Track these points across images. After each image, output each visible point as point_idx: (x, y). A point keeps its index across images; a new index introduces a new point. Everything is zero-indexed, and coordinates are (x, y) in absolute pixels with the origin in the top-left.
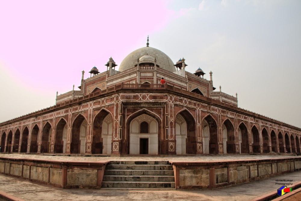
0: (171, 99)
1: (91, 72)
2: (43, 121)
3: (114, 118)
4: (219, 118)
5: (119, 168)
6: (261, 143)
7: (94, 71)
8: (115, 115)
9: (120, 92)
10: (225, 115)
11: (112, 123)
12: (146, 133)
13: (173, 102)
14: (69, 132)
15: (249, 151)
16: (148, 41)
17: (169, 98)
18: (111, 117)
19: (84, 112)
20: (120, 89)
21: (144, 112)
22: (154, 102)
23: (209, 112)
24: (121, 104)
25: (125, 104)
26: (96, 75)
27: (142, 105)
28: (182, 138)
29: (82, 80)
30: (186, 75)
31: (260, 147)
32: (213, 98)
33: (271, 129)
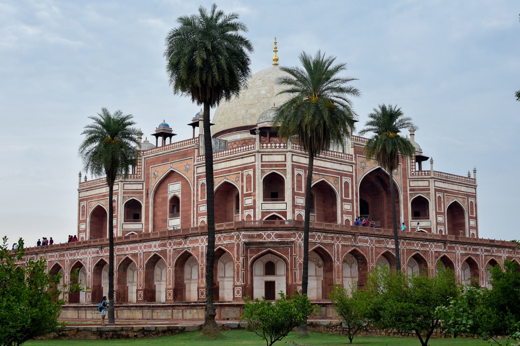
1: (157, 135)
4: (370, 252)
7: (165, 133)
8: (236, 256)
9: (242, 231)
10: (383, 245)
17: (297, 236)
19: (193, 249)
22: (281, 242)
23: (354, 246)
24: (243, 244)
25: (247, 244)
27: (267, 245)
28: (317, 280)
32: (413, 184)
33: (488, 257)
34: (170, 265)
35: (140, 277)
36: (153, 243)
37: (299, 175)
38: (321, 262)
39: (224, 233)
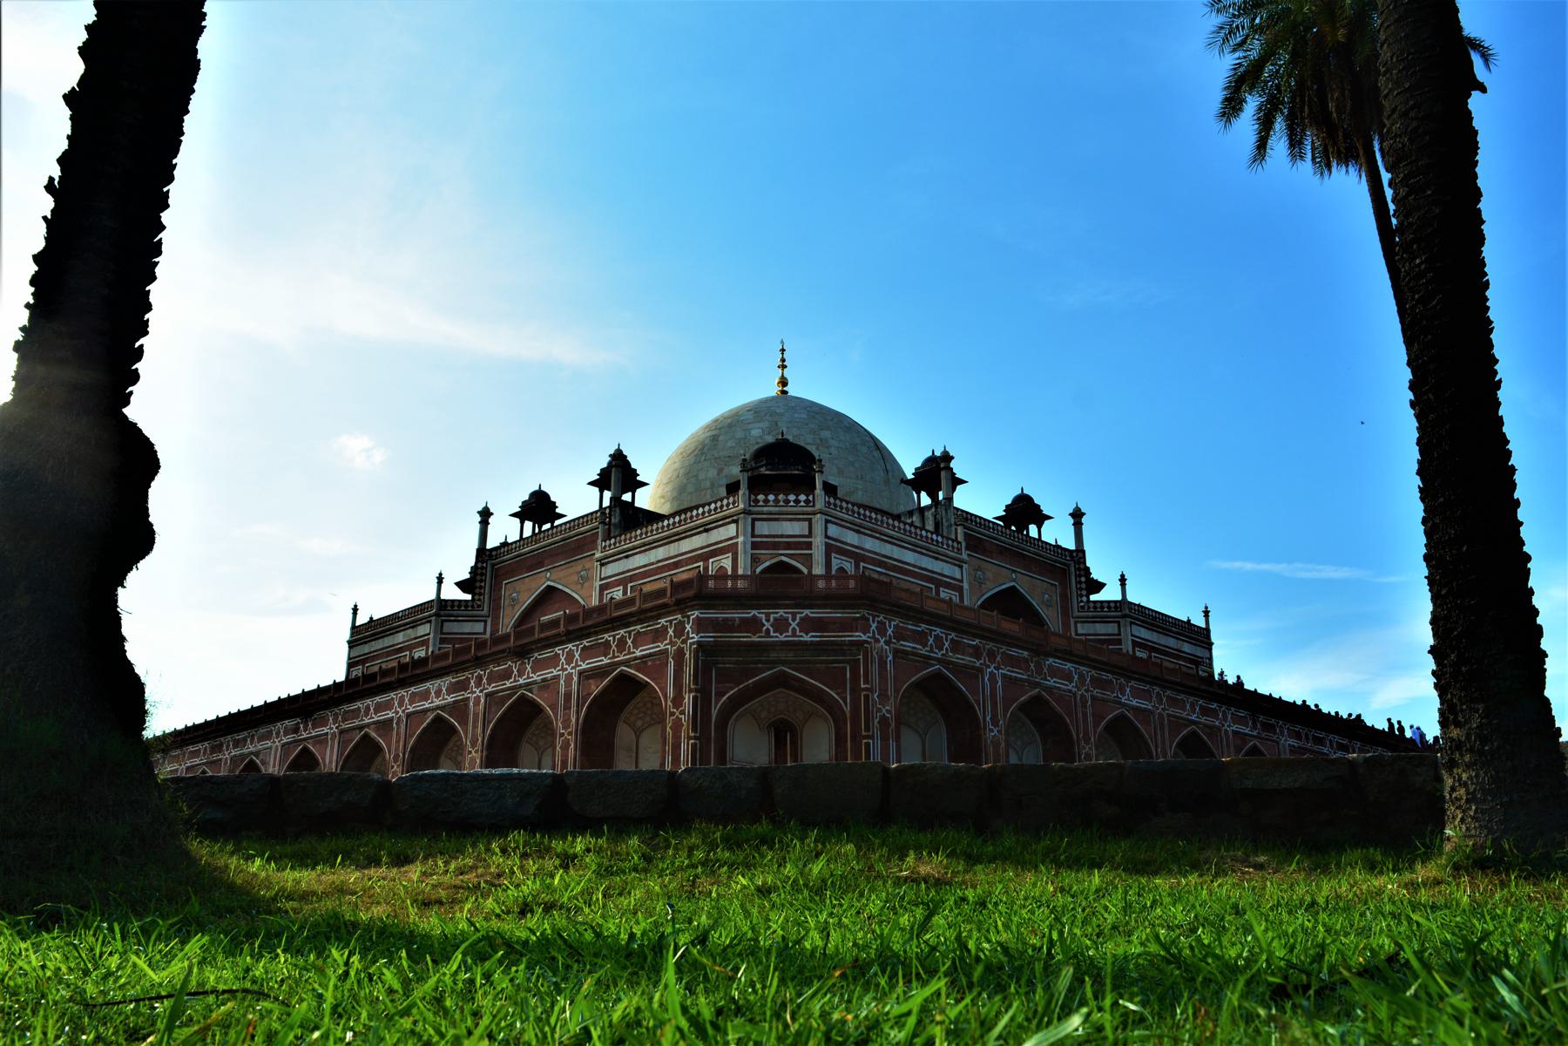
0: (882, 630)
2: (342, 732)
4: (1079, 709)
9: (693, 608)
11: (659, 727)
13: (888, 643)
17: (874, 626)
20: (695, 593)
21: (782, 681)
23: (1038, 685)
24: (696, 651)
26: (547, 526)
27: (773, 655)
30: (960, 529)
34: (474, 744)
37: (841, 569)
39: (635, 623)
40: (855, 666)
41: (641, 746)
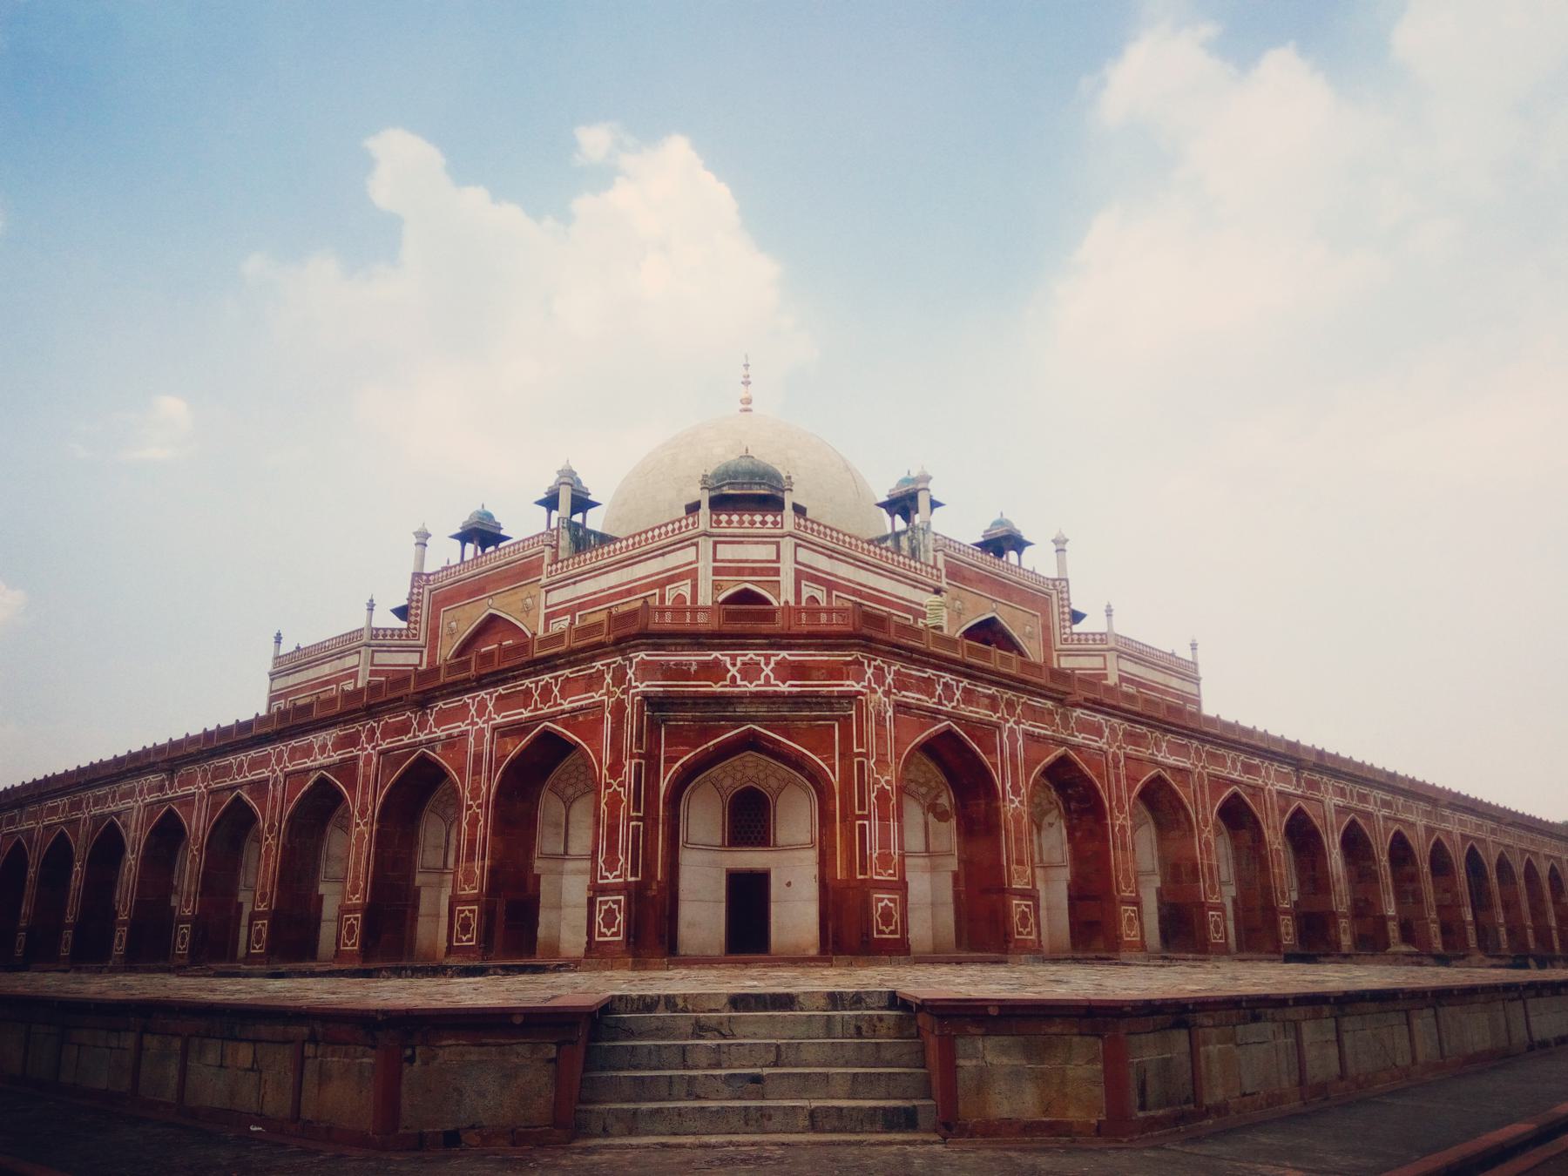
1: (465, 537)
2: (211, 792)
3: (605, 771)
4: (1112, 771)
5: (660, 1032)
6: (1341, 898)
7: (482, 534)
8: (607, 757)
9: (636, 648)
10: (1145, 753)
11: (592, 796)
12: (759, 845)
13: (887, 693)
14: (359, 847)
15: (1278, 941)
16: (747, 383)
17: (870, 672)
18: (582, 769)
19: (445, 747)
21: (751, 743)
23: (1063, 743)
24: (641, 704)
26: (492, 548)
27: (740, 710)
28: (933, 869)
29: (417, 576)
30: (940, 556)
31: (1336, 924)
32: (1066, 663)
33: (1390, 824)
34: (362, 814)
35: (267, 865)
36: (316, 739)
37: (813, 599)
38: (946, 800)
39: (563, 667)
40: (845, 722)
41: (572, 819)
